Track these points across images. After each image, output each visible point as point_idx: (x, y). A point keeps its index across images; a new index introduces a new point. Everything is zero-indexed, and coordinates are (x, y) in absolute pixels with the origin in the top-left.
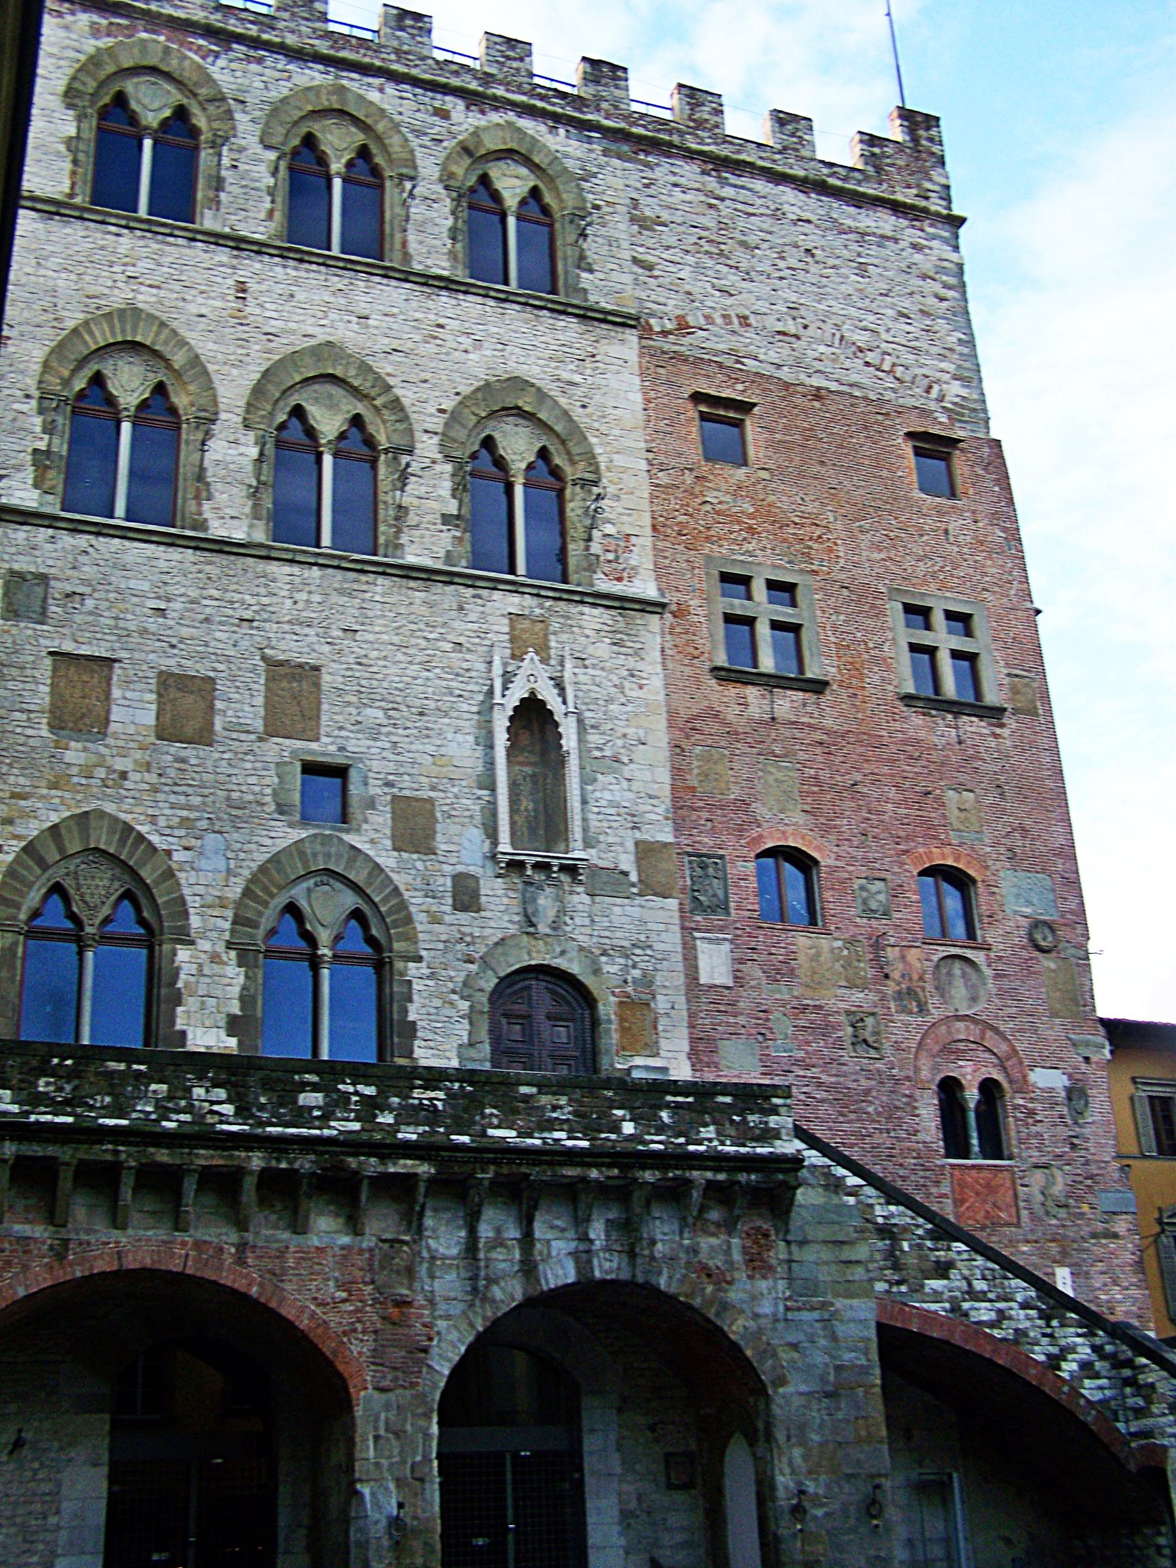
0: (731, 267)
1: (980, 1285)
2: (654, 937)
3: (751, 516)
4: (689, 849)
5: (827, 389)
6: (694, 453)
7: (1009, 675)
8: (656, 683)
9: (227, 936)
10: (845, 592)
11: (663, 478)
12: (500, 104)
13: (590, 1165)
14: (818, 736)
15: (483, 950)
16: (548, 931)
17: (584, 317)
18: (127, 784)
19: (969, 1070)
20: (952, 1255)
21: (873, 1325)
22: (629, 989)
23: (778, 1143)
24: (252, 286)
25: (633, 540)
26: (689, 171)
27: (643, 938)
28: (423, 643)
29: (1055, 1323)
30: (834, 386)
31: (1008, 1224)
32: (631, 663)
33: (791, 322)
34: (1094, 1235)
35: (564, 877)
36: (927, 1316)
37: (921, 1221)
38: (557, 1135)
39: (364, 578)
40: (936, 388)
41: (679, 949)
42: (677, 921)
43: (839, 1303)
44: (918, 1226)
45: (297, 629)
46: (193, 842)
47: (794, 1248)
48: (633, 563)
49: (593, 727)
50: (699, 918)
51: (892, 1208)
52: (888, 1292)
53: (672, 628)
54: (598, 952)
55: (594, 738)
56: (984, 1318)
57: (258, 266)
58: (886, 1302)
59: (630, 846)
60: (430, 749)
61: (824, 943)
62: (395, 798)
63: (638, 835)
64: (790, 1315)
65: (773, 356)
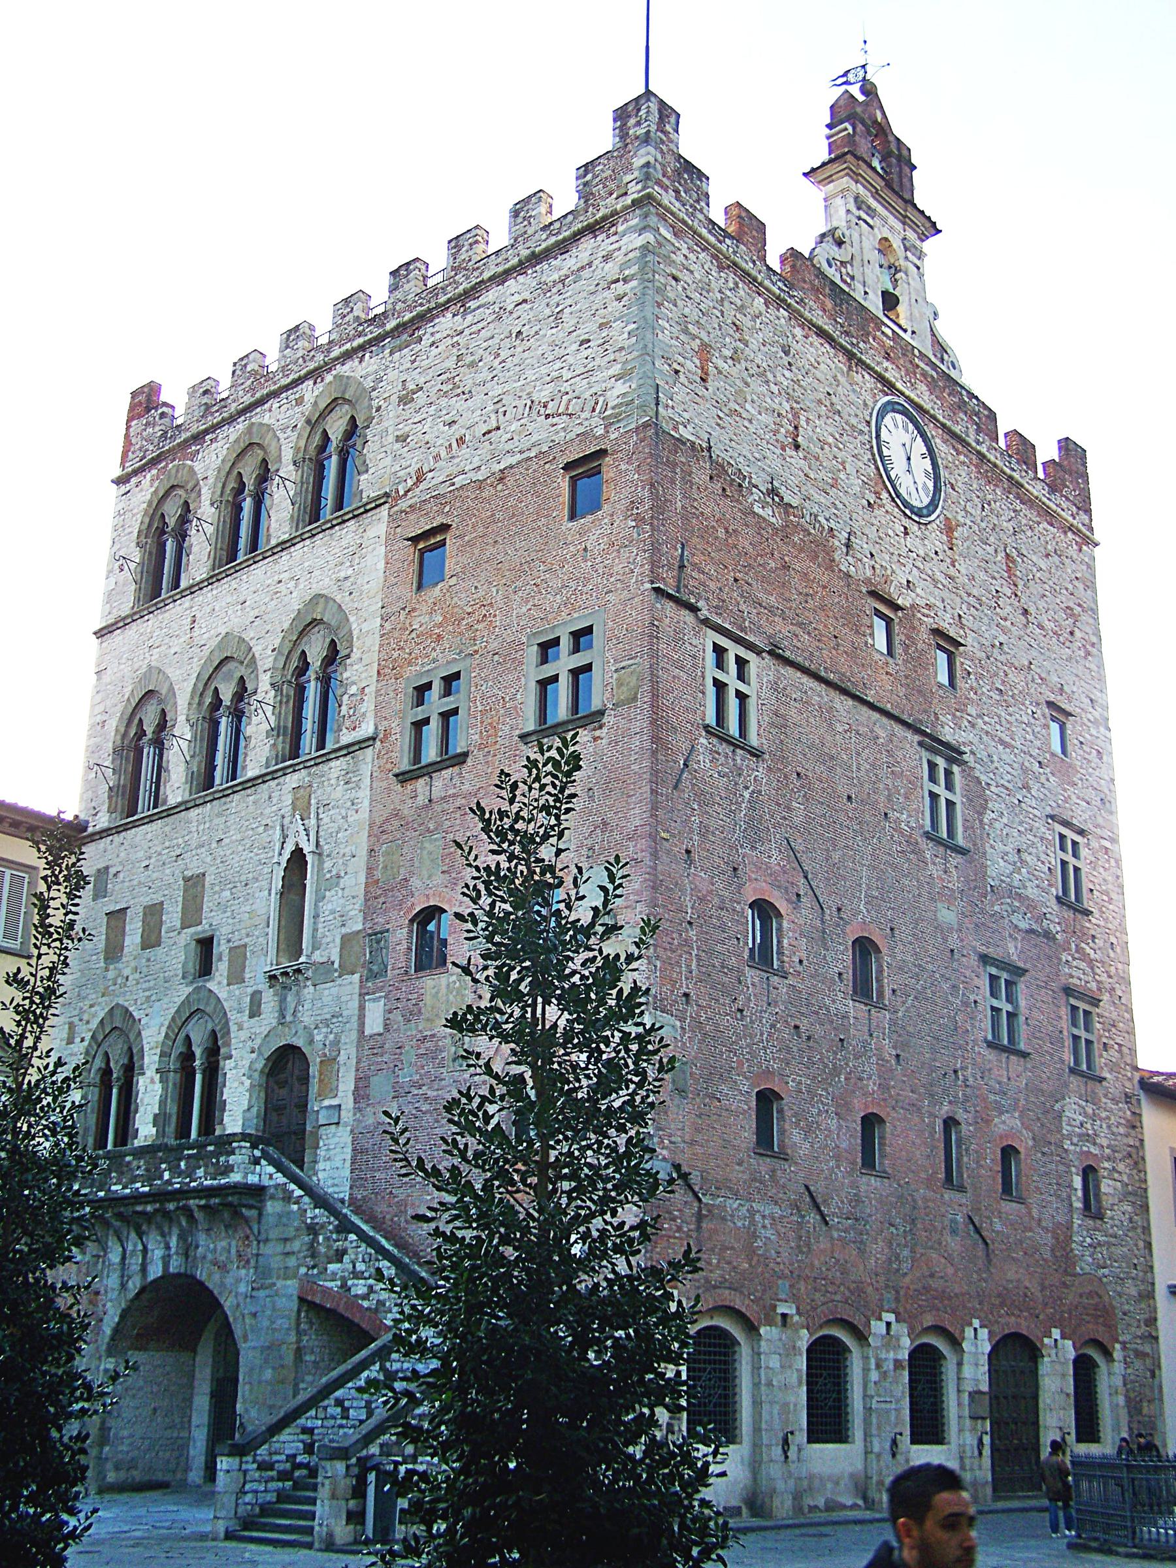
0: (458, 395)
1: (360, 1267)
2: (344, 1007)
3: (440, 625)
4: (370, 931)
5: (511, 467)
6: (406, 591)
7: (616, 671)
8: (366, 803)
9: (157, 1066)
11: (388, 626)
12: (327, 367)
13: (147, 1203)
14: (458, 804)
15: (258, 1041)
17: (355, 517)
18: (128, 983)
20: (347, 1244)
21: (295, 1298)
22: (327, 1051)
23: (232, 1175)
25: (367, 690)
26: (446, 323)
27: (337, 1009)
28: (251, 832)
30: (513, 460)
32: (354, 794)
33: (493, 416)
35: (300, 977)
36: (326, 1291)
37: (332, 1219)
38: (138, 1185)
39: (228, 799)
40: (601, 399)
41: (356, 1012)
42: (357, 990)
44: (330, 1223)
45: (199, 851)
46: (149, 1011)
47: (262, 1244)
48: (363, 710)
49: (328, 856)
50: (370, 984)
51: (317, 1211)
52: (306, 1274)
53: (380, 752)
54: (313, 1027)
55: (328, 864)
56: (360, 1292)
57: (201, 598)
58: (308, 1283)
59: (338, 941)
60: (248, 908)
62: (231, 949)
64: (254, 1293)
65: (476, 462)
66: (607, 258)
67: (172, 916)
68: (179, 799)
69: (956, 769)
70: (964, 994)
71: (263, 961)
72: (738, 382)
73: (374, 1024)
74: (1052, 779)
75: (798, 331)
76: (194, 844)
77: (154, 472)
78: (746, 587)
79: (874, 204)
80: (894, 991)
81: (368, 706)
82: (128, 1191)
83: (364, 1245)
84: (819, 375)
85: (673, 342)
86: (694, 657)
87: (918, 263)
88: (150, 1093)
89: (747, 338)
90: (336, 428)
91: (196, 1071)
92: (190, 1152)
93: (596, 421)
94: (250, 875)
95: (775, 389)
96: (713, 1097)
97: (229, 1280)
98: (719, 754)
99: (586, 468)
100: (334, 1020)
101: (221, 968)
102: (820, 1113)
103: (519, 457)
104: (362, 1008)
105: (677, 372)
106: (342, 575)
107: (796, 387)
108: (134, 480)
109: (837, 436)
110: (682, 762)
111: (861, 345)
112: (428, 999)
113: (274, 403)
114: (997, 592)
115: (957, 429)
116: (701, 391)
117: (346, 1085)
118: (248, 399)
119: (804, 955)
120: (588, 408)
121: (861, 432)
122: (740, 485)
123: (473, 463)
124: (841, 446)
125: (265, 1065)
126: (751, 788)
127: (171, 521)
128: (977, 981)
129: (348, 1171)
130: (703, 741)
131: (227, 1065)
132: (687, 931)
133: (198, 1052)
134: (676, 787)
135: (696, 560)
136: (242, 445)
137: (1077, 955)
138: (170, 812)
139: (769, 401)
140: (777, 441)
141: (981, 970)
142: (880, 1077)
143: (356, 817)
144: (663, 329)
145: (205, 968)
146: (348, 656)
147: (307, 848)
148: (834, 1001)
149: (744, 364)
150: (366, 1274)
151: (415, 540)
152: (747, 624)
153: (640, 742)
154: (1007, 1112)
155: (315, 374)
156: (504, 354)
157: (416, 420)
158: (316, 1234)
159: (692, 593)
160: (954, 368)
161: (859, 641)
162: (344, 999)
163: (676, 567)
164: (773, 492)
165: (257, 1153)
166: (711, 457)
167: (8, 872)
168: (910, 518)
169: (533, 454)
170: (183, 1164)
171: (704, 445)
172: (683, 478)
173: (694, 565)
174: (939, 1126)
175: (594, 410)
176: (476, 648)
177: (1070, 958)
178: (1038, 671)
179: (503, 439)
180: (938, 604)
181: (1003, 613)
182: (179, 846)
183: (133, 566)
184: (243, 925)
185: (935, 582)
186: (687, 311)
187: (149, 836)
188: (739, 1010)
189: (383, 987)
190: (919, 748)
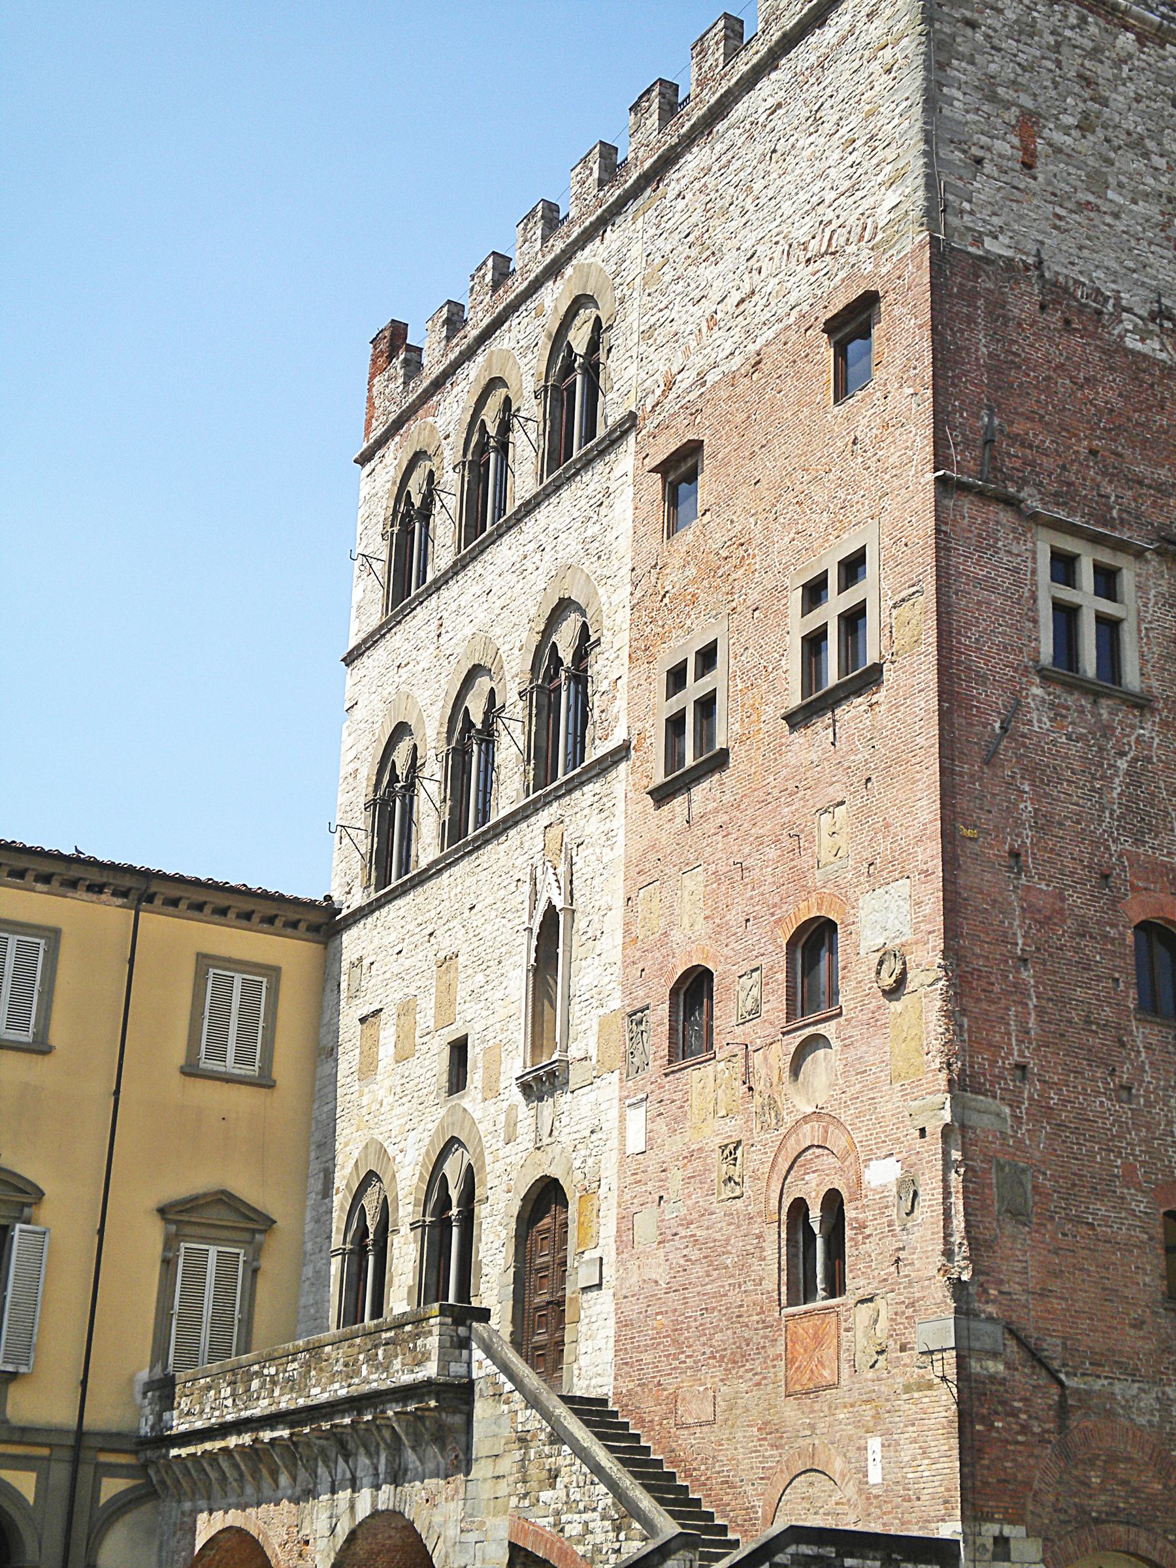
1: (576, 1495)
2: (603, 1119)
4: (628, 1010)
5: (768, 344)
6: (654, 542)
10: (757, 614)
14: (719, 822)
15: (514, 1175)
16: (549, 1140)
18: (383, 1110)
19: (814, 1184)
24: (445, 615)
26: (694, 160)
29: (622, 1536)
30: (770, 334)
31: (829, 1387)
33: (746, 277)
34: (907, 1389)
38: (336, 1386)
41: (617, 1124)
42: (617, 1094)
43: (490, 1521)
55: (581, 923)
58: (520, 1520)
59: (596, 1028)
60: (499, 995)
61: (709, 1069)
63: (601, 1011)
65: (728, 347)
66: (870, 16)
67: (426, 1017)
68: (431, 859)
71: (515, 1064)
72: (1091, 161)
73: (636, 1143)
76: (446, 915)
77: (397, 438)
78: (1111, 459)
81: (620, 704)
82: (326, 1395)
83: (578, 1461)
85: (970, 117)
86: (1016, 570)
88: (405, 1255)
89: (1107, 94)
90: (579, 339)
91: (449, 1219)
92: (391, 1334)
93: (866, 252)
94: (503, 950)
95: (1161, 163)
96: (1079, 1221)
97: (437, 1519)
99: (853, 324)
100: (594, 1137)
101: (475, 1077)
103: (778, 327)
104: (622, 1118)
105: (979, 161)
106: (589, 533)
108: (378, 455)
110: (997, 725)
112: (695, 1100)
113: (514, 321)
116: (1024, 182)
117: (608, 1228)
118: (487, 321)
120: (854, 238)
122: (1099, 313)
123: (725, 349)
125: (522, 1208)
126: (1132, 754)
127: (417, 500)
129: (612, 1353)
130: (1038, 691)
131: (481, 1211)
132: (1018, 971)
133: (454, 1194)
134: (987, 762)
135: (1017, 429)
136: (483, 382)
138: (424, 877)
139: (1151, 181)
140: (1168, 239)
143: (611, 855)
144: (950, 101)
145: (457, 1079)
146: (598, 642)
147: (559, 903)
150: (581, 1506)
151: (663, 468)
152: (1115, 513)
153: (928, 702)
155: (553, 270)
156: (758, 186)
157: (662, 306)
158: (527, 1448)
159: (1010, 478)
162: (604, 1107)
163: (980, 442)
164: (1160, 314)
165: (462, 1331)
166: (1042, 276)
167: (238, 978)
169: (792, 319)
170: (380, 1352)
171: (1030, 260)
172: (989, 313)
173: (1014, 438)
175: (861, 238)
176: (734, 604)
179: (758, 308)
182: (430, 921)
183: (378, 566)
184: (497, 1017)
186: (993, 67)
187: (401, 913)
188: (1122, 1087)
189: (644, 1086)
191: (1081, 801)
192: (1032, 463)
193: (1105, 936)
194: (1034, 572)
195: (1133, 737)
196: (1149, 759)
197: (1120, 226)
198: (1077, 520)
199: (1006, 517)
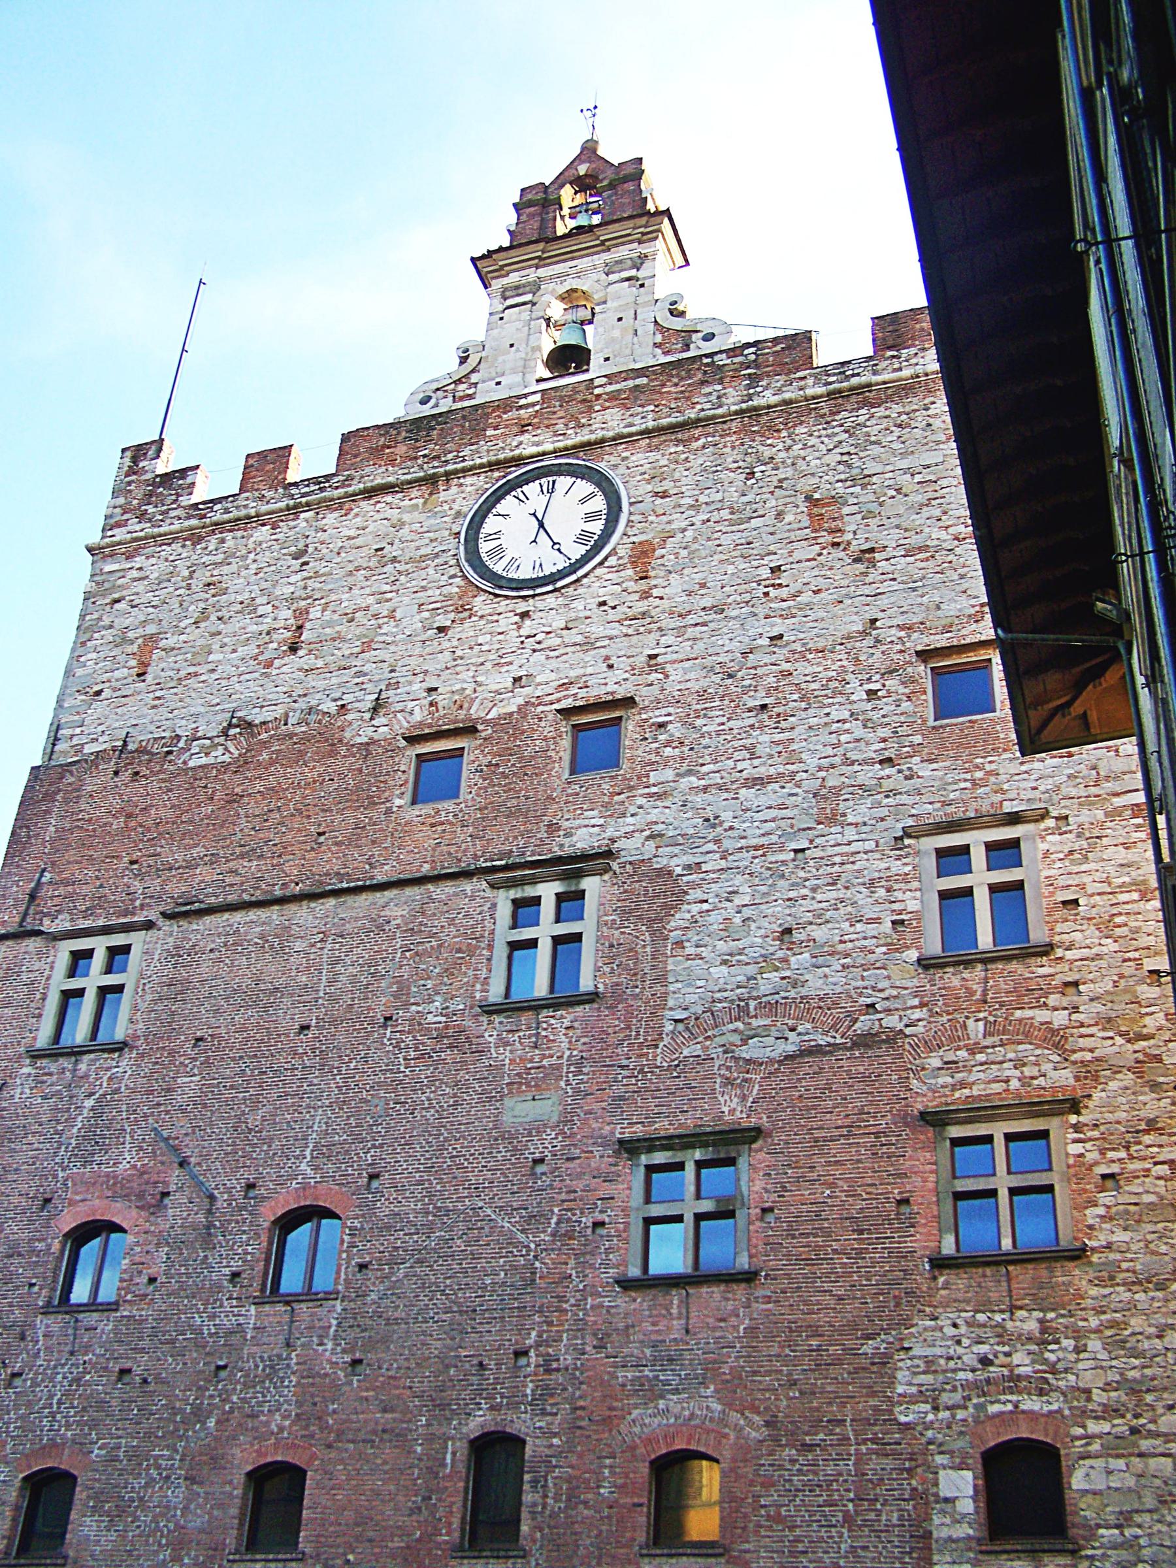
69: (590, 884)
70: (557, 1224)
74: (925, 771)
75: (331, 518)
79: (533, 274)
80: (362, 1267)
84: (358, 542)
87: (633, 273)
98: (50, 1074)
102: (150, 1483)
107: (309, 582)
109: (387, 588)
111: (466, 452)
114: (776, 570)
115: (692, 414)
119: (157, 1268)
121: (437, 555)
124: (389, 596)
128: (606, 1190)
137: (989, 1041)
141: (624, 1166)
142: (299, 1404)
148: (213, 1317)
149: (213, 618)
152: (138, 903)
154: (676, 1391)
160: (709, 337)
161: (377, 813)
168: (533, 596)
174: (455, 1455)
177: (963, 1054)
178: (899, 621)
180: (589, 670)
181: (784, 593)
185: (587, 645)
188: (15, 1375)
190: (489, 893)
191: (41, 1146)
192: (69, 896)
193: (33, 1251)
194: (48, 979)
195: (105, 1078)
196: (117, 1091)
197: (215, 676)
198: (101, 923)
199: (33, 944)
